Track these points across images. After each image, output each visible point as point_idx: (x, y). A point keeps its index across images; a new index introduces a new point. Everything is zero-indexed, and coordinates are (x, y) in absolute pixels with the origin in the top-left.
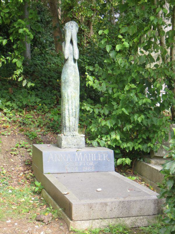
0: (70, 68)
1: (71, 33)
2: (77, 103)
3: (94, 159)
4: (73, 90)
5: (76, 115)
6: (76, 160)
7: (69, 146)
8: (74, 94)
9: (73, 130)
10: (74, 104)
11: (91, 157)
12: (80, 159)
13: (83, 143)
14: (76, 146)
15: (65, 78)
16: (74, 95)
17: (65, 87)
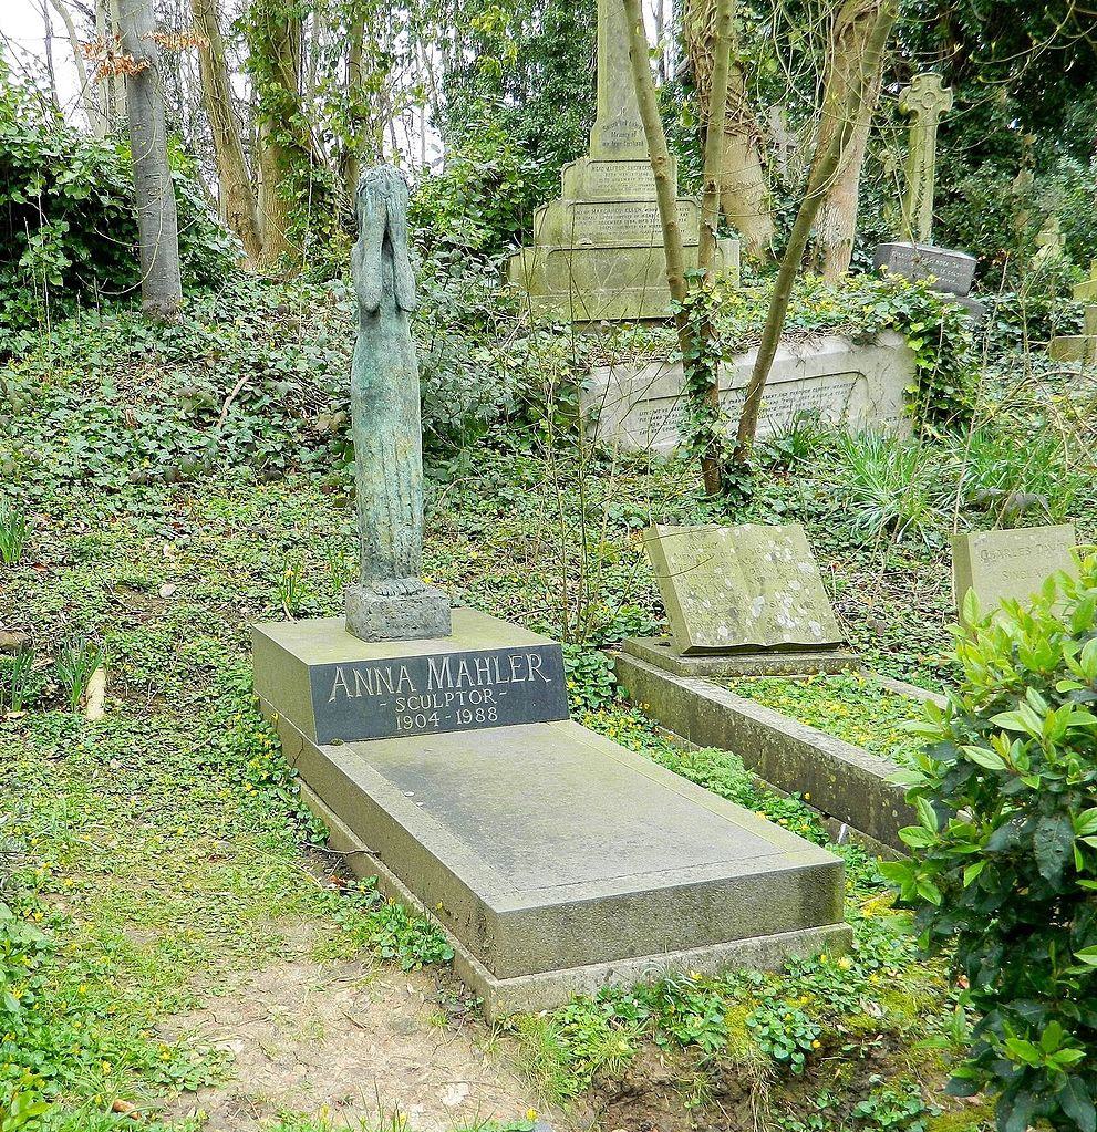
0: (384, 342)
1: (383, 210)
3: (494, 678)
7: (395, 630)
11: (484, 674)
16: (402, 442)
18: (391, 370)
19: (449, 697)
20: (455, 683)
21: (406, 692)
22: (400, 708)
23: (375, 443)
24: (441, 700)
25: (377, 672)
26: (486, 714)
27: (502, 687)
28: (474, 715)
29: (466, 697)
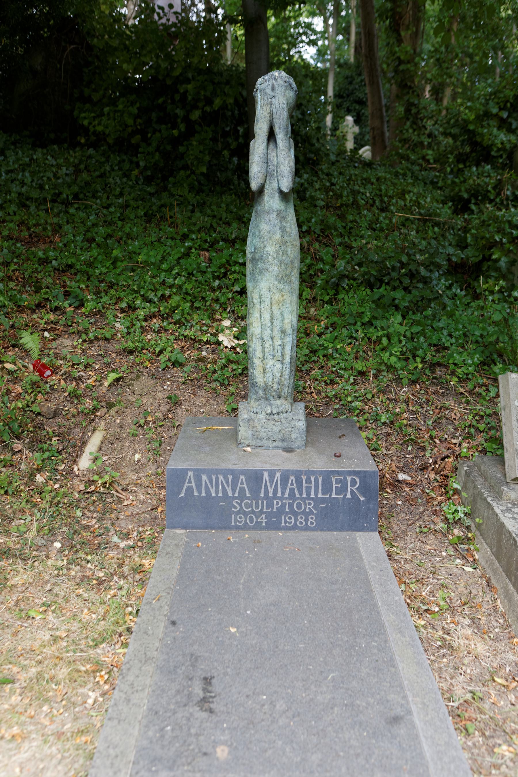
2: (286, 321)
3: (316, 493)
4: (276, 283)
5: (283, 355)
6: (262, 495)
7: (258, 441)
8: (278, 294)
9: (276, 397)
10: (277, 323)
11: (308, 489)
12: (275, 492)
13: (298, 435)
14: (280, 444)
15: (255, 249)
16: (277, 296)
17: (253, 275)
18: (271, 239)
19: (277, 505)
20: (283, 493)
21: (242, 496)
22: (236, 508)
23: (256, 296)
24: (270, 505)
25: (221, 478)
26: (307, 520)
27: (323, 500)
28: (296, 520)
29: (291, 505)
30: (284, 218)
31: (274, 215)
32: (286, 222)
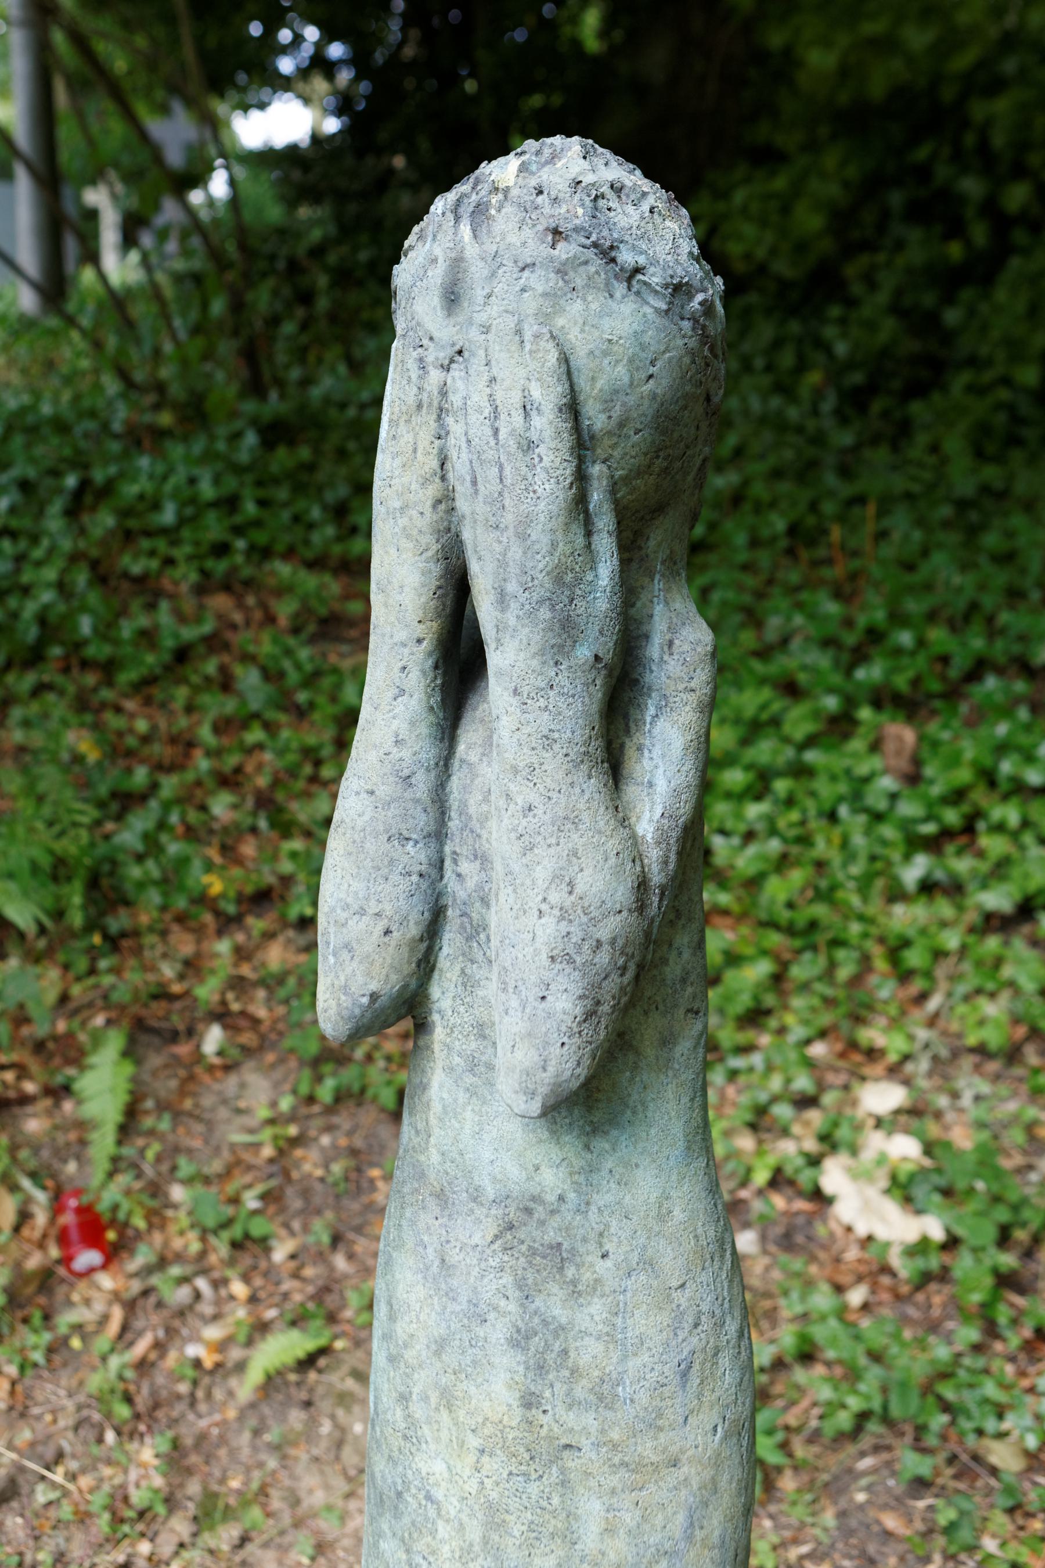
30: (558, 1257)
31: (478, 1229)
32: (575, 1292)
